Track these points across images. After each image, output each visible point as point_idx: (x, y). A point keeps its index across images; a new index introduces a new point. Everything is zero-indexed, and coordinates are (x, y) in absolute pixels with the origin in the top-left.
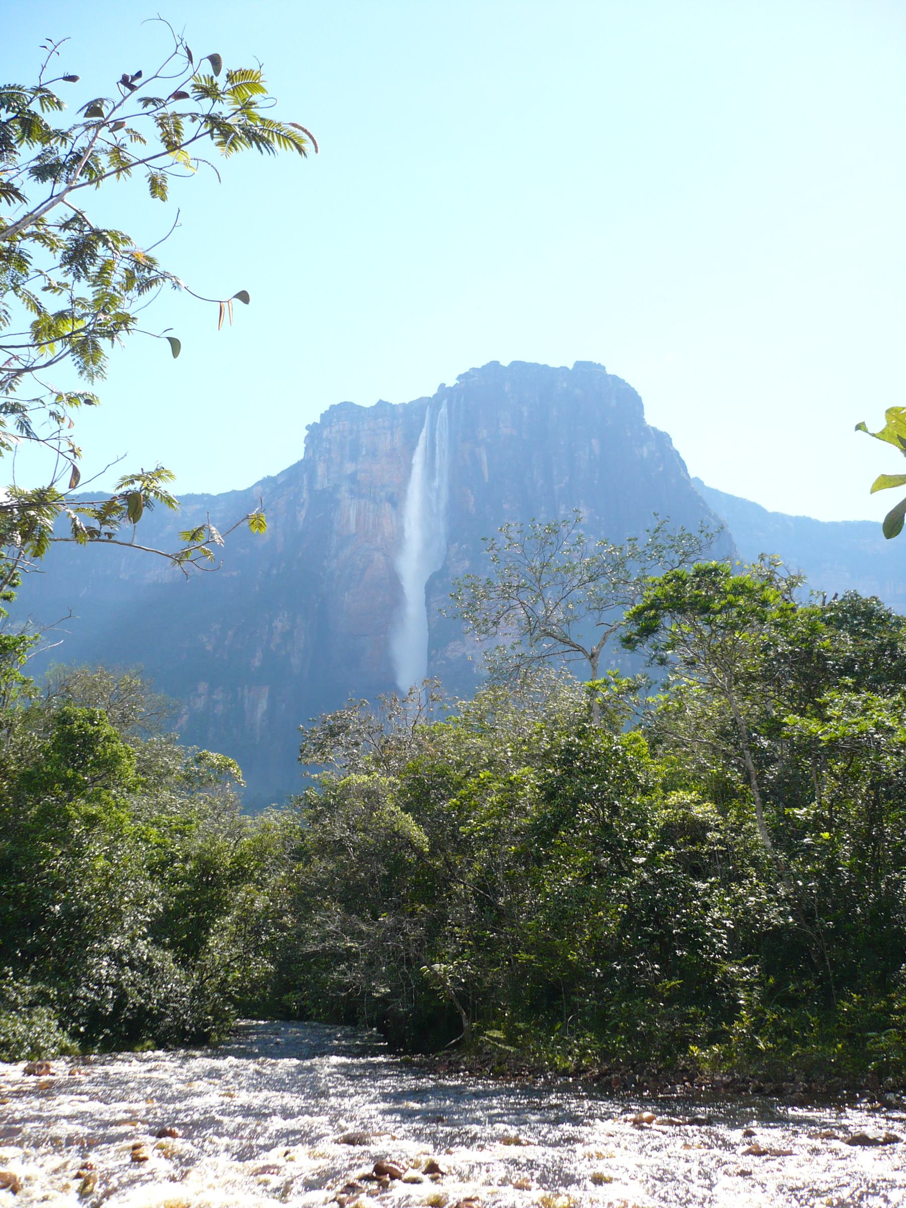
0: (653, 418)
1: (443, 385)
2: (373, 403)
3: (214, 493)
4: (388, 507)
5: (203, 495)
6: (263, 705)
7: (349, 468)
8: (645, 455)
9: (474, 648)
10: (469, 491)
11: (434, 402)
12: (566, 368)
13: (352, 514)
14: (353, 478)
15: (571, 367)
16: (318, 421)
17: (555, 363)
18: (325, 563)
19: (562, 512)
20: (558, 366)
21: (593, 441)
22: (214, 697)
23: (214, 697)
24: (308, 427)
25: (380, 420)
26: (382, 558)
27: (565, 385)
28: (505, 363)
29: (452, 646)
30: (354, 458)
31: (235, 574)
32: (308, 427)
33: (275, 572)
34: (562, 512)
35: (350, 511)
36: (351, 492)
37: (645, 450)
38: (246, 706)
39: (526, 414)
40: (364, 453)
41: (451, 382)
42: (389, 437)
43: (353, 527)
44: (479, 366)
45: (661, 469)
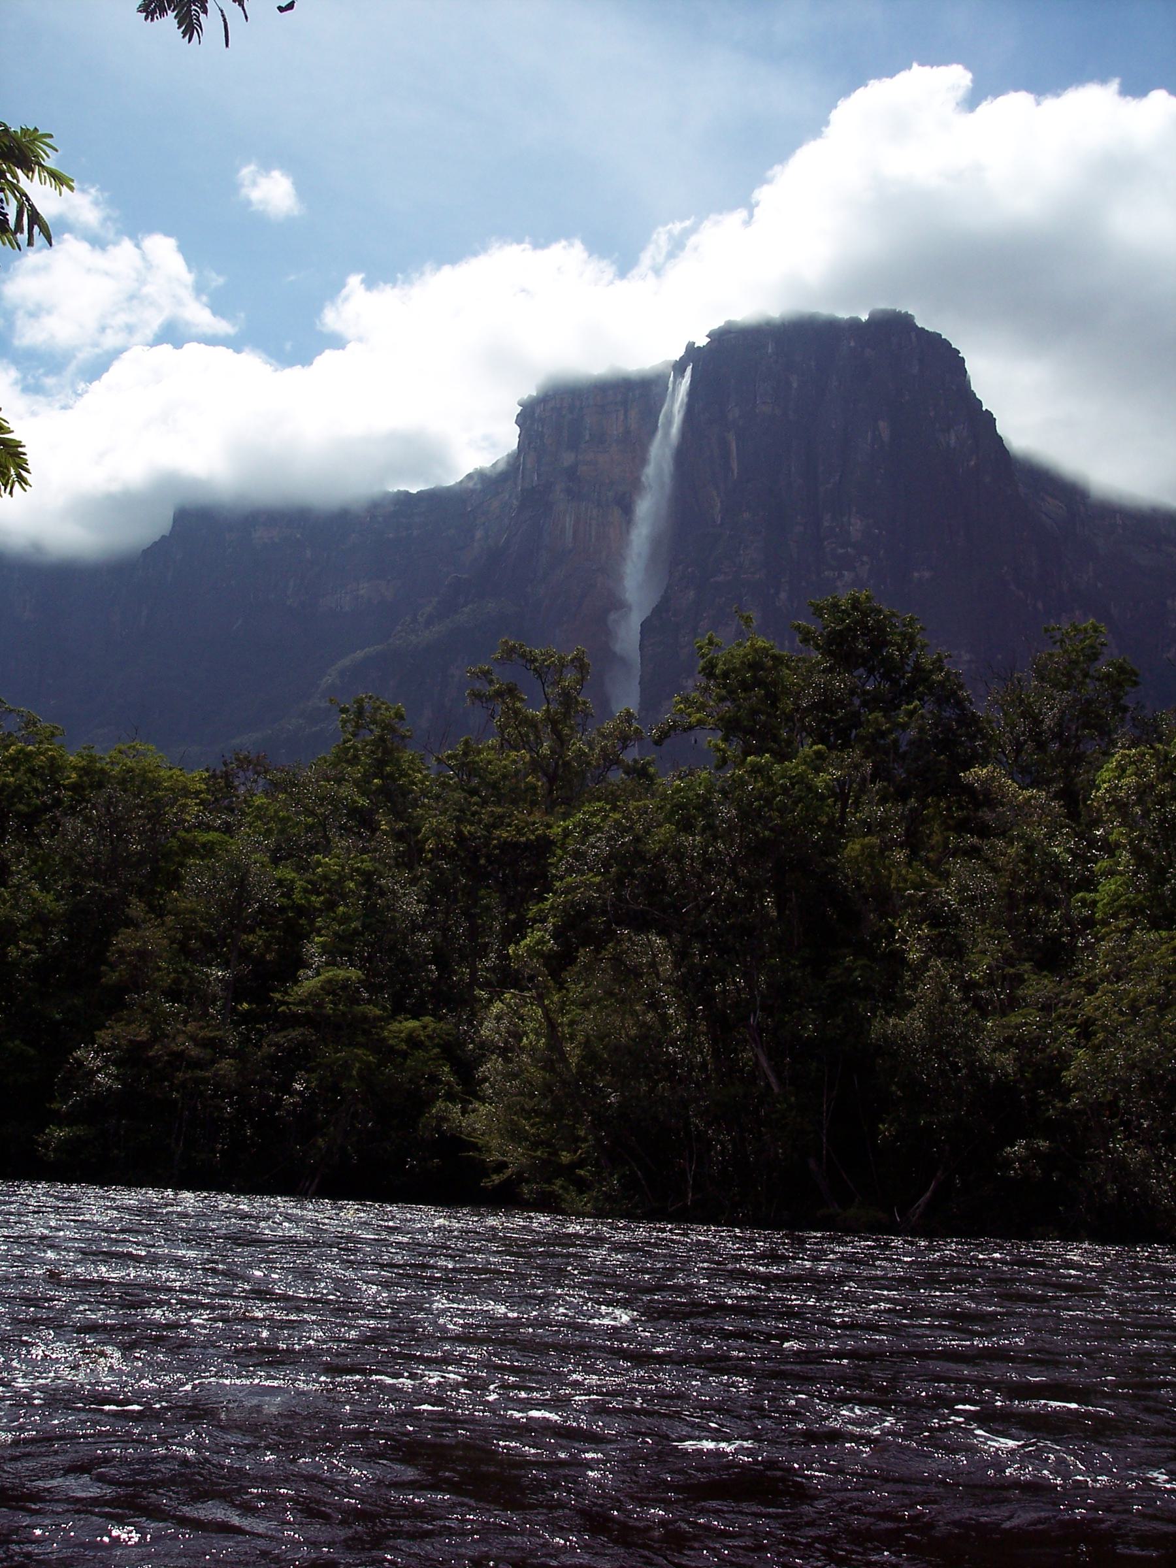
7: (568, 458)
8: (953, 442)
13: (569, 521)
14: (571, 473)
19: (826, 524)
21: (881, 424)
27: (852, 344)
34: (826, 524)
37: (953, 437)
39: (795, 385)
40: (587, 438)
41: (702, 341)
45: (972, 463)
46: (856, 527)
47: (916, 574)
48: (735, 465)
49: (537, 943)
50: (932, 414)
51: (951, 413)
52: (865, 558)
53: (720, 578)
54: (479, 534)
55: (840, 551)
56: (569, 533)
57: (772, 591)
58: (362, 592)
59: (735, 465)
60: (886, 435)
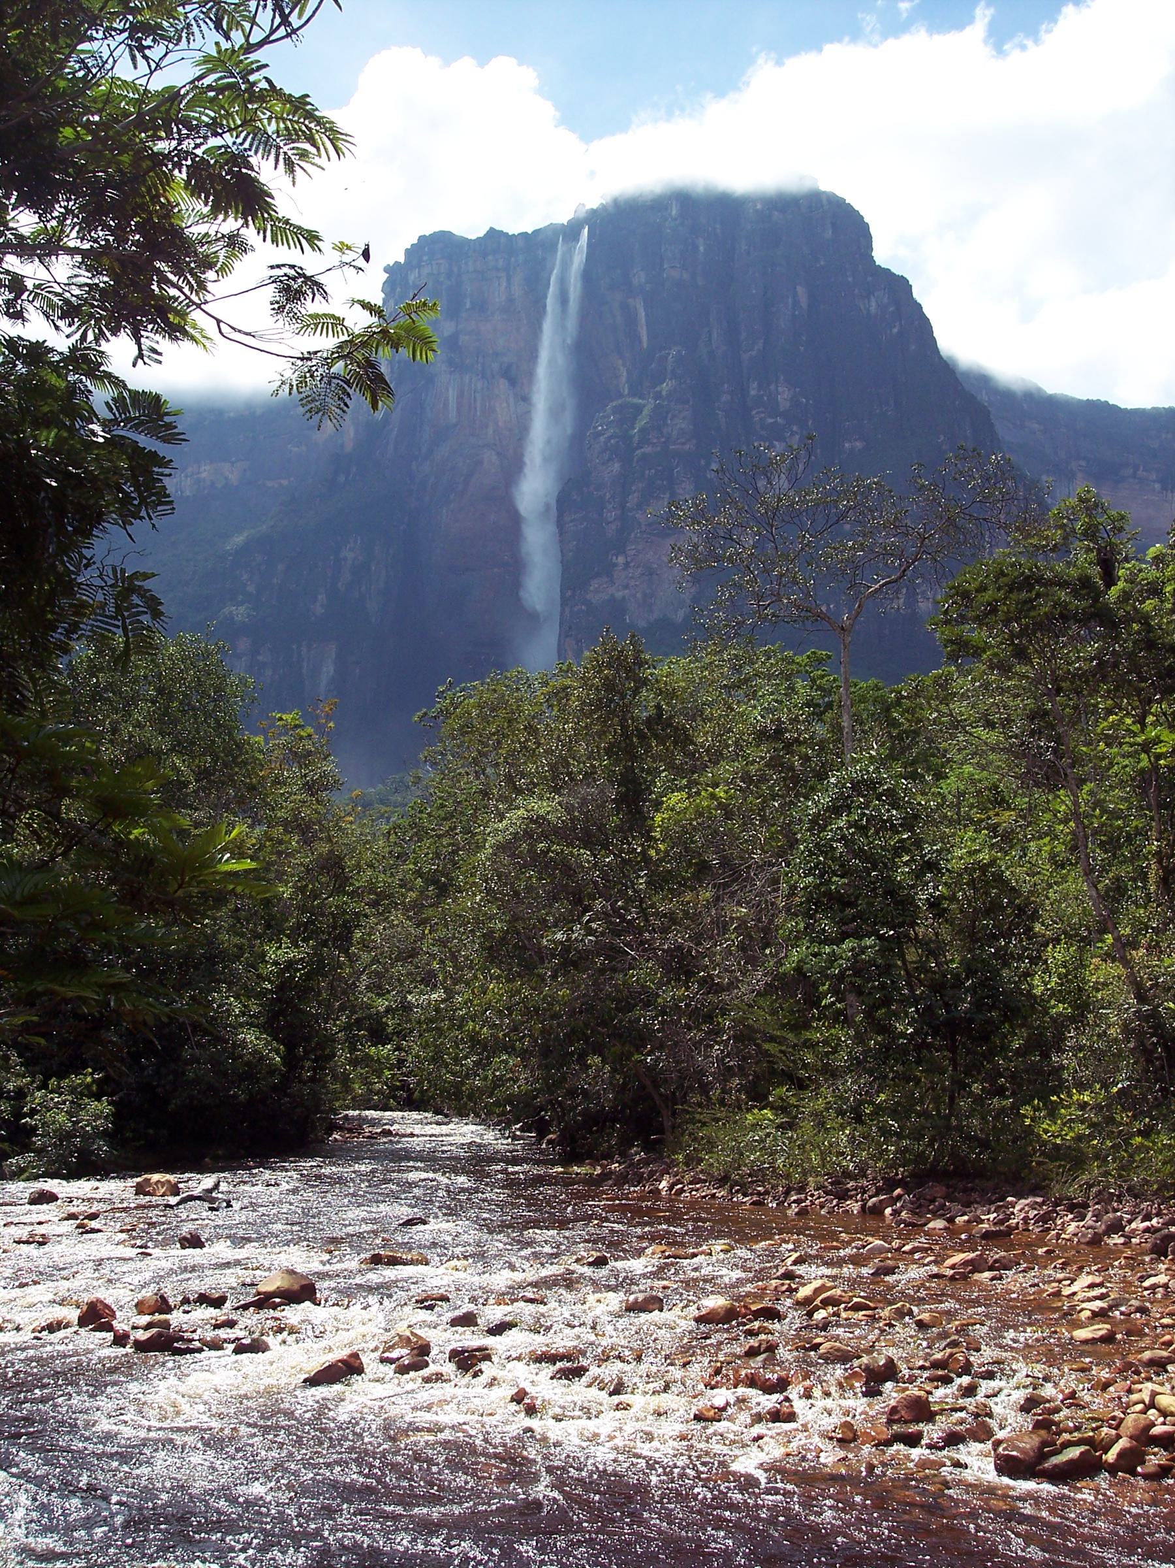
0: (883, 254)
4: (503, 384)
6: (329, 669)
9: (626, 587)
10: (620, 362)
11: (571, 231)
13: (452, 395)
16: (402, 260)
18: (414, 467)
19: (753, 393)
22: (260, 658)
23: (260, 658)
24: (386, 270)
25: (490, 257)
26: (494, 458)
29: (595, 584)
31: (285, 483)
32: (386, 270)
33: (342, 479)
34: (753, 393)
36: (450, 362)
37: (874, 304)
38: (304, 671)
39: (702, 249)
40: (468, 305)
43: (453, 416)
45: (895, 330)
46: (784, 395)
47: (847, 445)
50: (850, 279)
51: (869, 279)
52: (795, 428)
53: (647, 449)
55: (770, 421)
57: (703, 462)
58: (204, 475)
60: (804, 302)
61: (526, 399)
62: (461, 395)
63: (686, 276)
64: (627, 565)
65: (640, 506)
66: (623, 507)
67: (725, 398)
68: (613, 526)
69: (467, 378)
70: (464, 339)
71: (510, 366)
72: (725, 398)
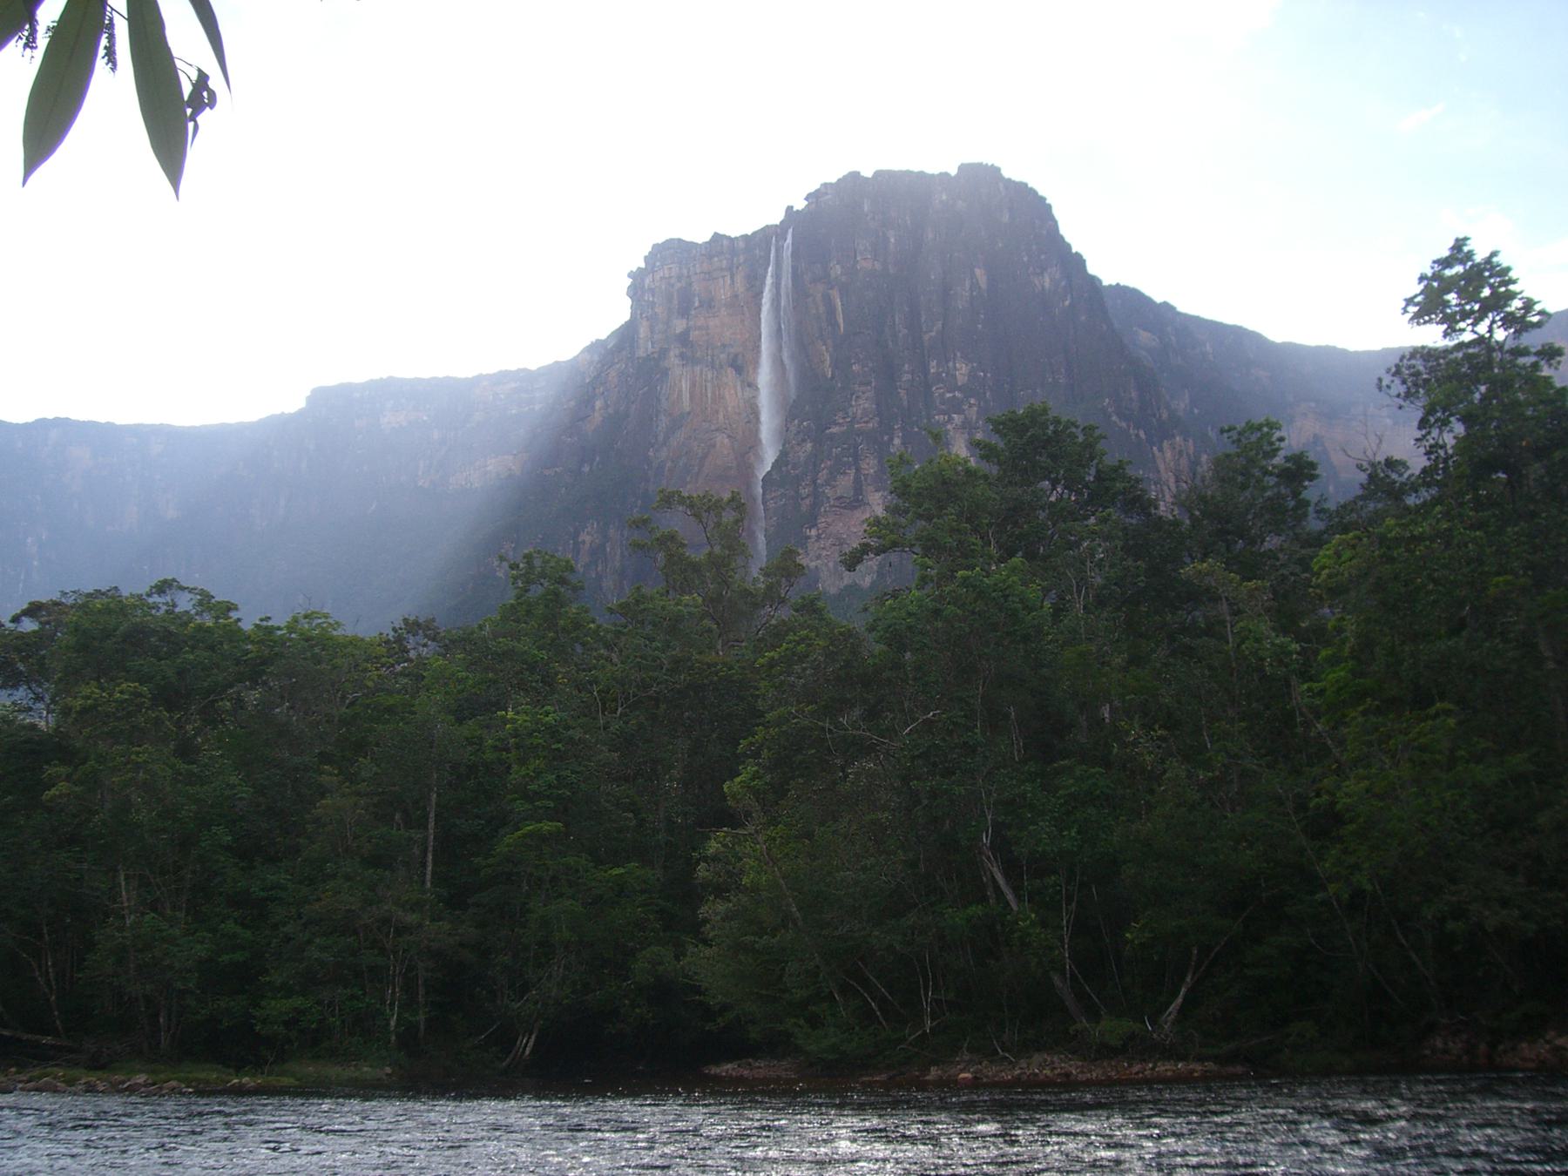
1: (790, 209)
2: (706, 237)
3: (533, 367)
4: (730, 370)
5: (519, 371)
7: (679, 325)
8: (1047, 285)
9: (819, 557)
12: (946, 174)
13: (685, 386)
14: (683, 339)
15: (953, 172)
16: (643, 265)
17: (933, 167)
18: (651, 454)
20: (936, 172)
21: (978, 272)
28: (868, 173)
30: (684, 312)
32: (629, 276)
33: (586, 469)
35: (682, 381)
36: (682, 356)
37: (1047, 280)
41: (800, 204)
42: (728, 280)
44: (834, 180)
46: (962, 371)
48: (841, 321)
49: (753, 779)
53: (835, 430)
54: (598, 404)
56: (686, 396)
59: (841, 321)
60: (983, 282)
61: (752, 385)
62: (693, 385)
63: (878, 266)
64: (819, 537)
65: (827, 483)
66: (814, 482)
67: (906, 377)
68: (807, 501)
69: (698, 369)
70: (694, 335)
71: (736, 355)
72: (906, 377)
